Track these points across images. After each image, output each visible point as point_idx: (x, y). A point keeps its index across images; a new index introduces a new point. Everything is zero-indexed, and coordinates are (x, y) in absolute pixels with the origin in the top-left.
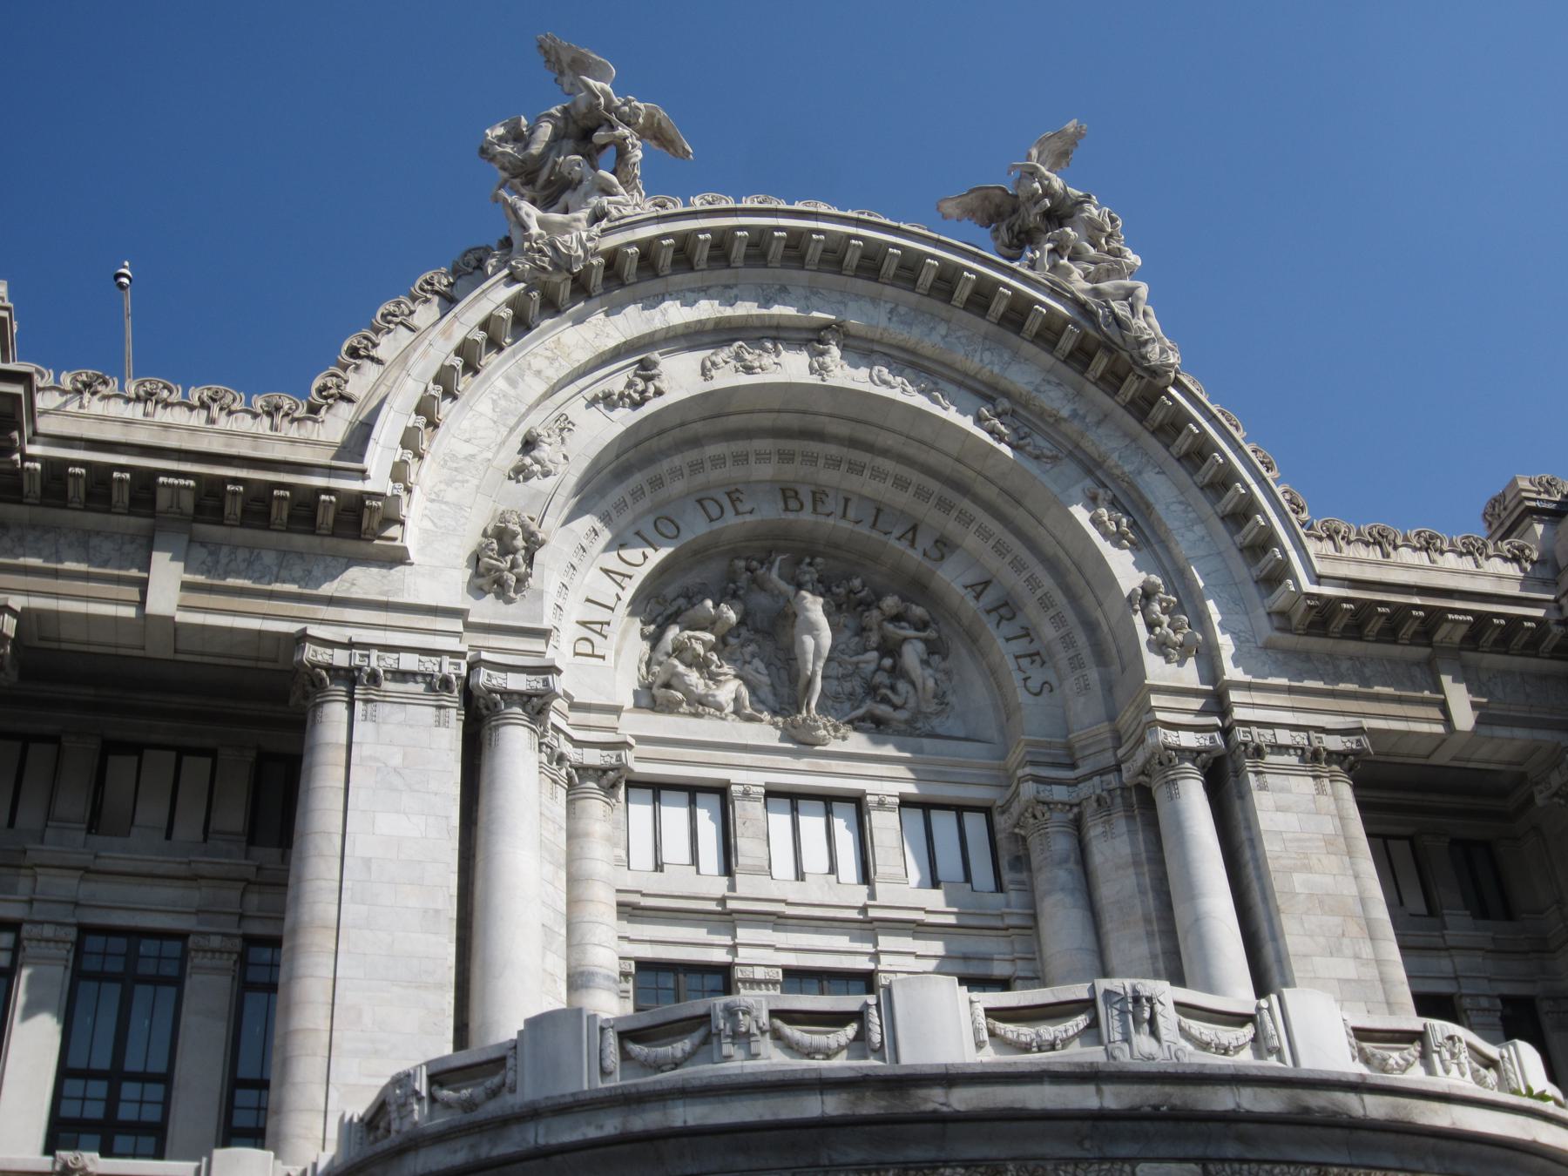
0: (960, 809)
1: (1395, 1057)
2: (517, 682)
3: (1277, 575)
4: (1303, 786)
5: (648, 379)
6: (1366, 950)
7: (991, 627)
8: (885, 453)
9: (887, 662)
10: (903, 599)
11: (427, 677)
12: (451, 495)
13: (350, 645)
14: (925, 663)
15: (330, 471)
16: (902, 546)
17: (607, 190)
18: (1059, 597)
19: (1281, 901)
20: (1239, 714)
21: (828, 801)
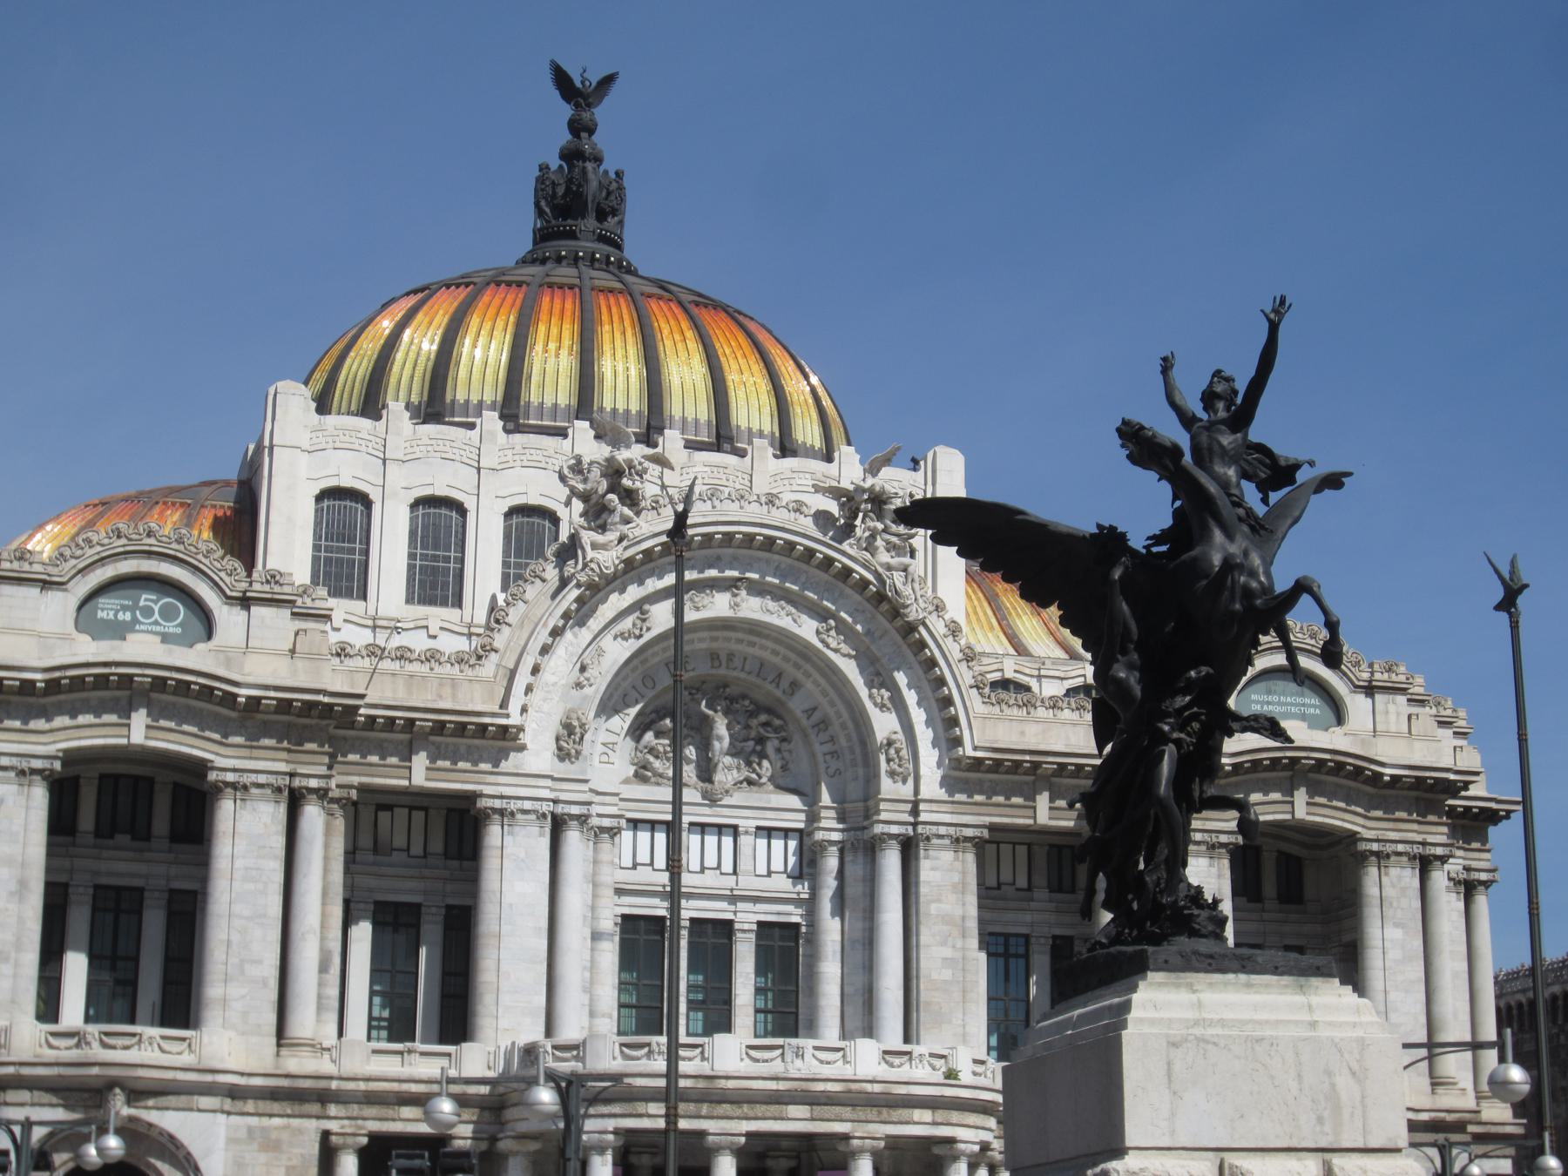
0: (786, 833)
1: (897, 1061)
2: (575, 810)
3: (958, 742)
4: (947, 856)
5: (644, 620)
6: (959, 944)
7: (813, 737)
8: (767, 637)
9: (758, 748)
10: (769, 711)
11: (535, 811)
12: (546, 707)
13: (502, 797)
14: (778, 750)
15: (493, 715)
16: (770, 687)
17: (627, 521)
18: (850, 725)
19: (922, 919)
20: (923, 817)
21: (720, 829)
